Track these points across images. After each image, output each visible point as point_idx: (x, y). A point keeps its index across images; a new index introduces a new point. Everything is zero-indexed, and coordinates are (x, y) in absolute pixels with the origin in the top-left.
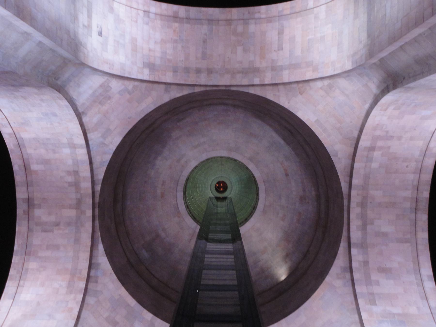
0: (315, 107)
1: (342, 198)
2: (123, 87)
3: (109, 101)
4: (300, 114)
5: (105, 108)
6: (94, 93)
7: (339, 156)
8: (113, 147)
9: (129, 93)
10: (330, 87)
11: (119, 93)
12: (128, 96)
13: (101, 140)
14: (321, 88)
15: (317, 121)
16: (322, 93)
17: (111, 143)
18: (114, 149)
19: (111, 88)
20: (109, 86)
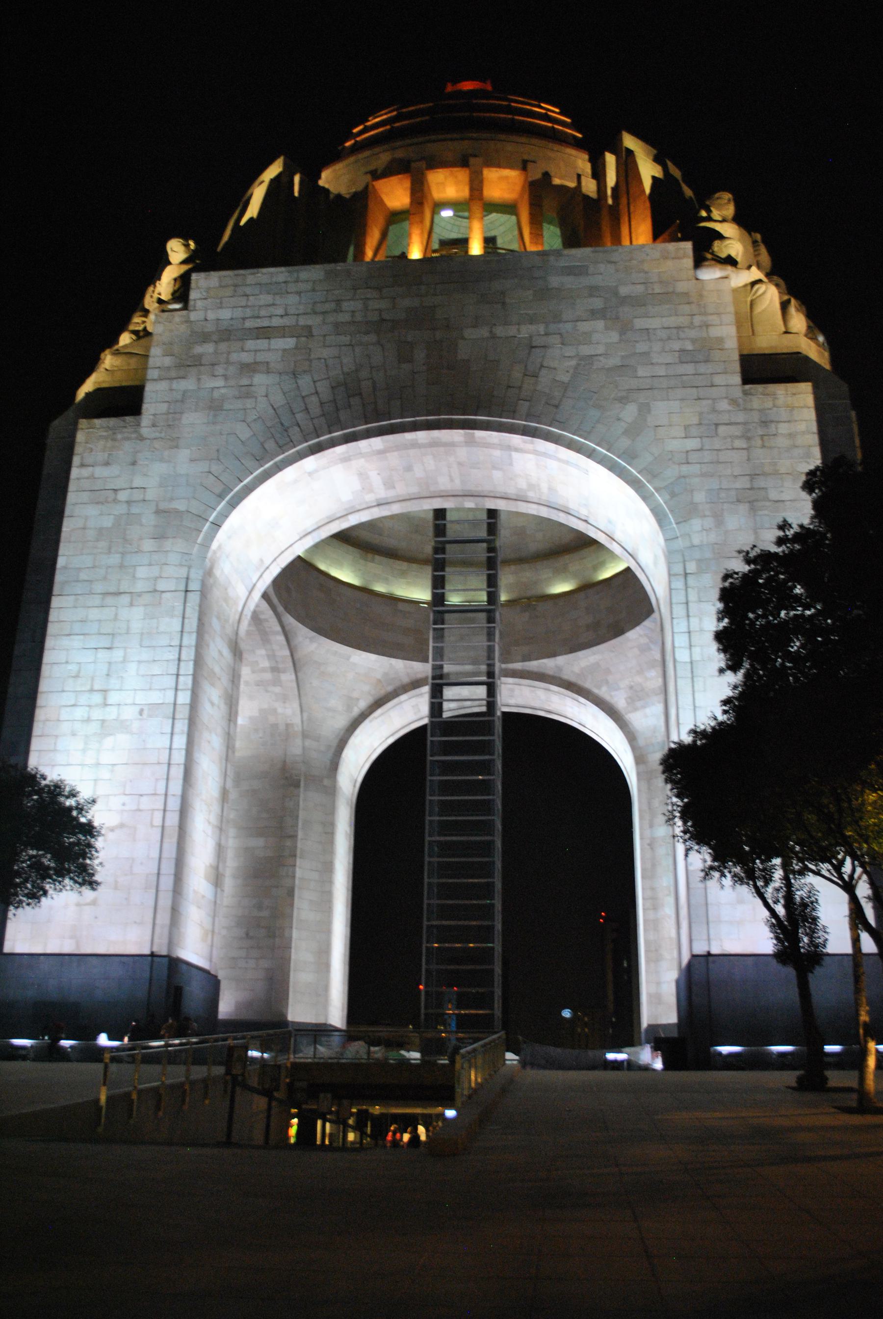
0: (356, 673)
1: (286, 608)
2: (613, 693)
3: (632, 684)
4: (373, 657)
5: (639, 679)
6: (644, 707)
7: (308, 640)
8: (638, 629)
9: (607, 682)
10: (349, 708)
11: (618, 689)
12: (610, 678)
13: (652, 646)
14: (358, 699)
15: (348, 658)
16: (355, 695)
17: (641, 636)
18: (638, 628)
19: (626, 699)
20: (628, 703)
